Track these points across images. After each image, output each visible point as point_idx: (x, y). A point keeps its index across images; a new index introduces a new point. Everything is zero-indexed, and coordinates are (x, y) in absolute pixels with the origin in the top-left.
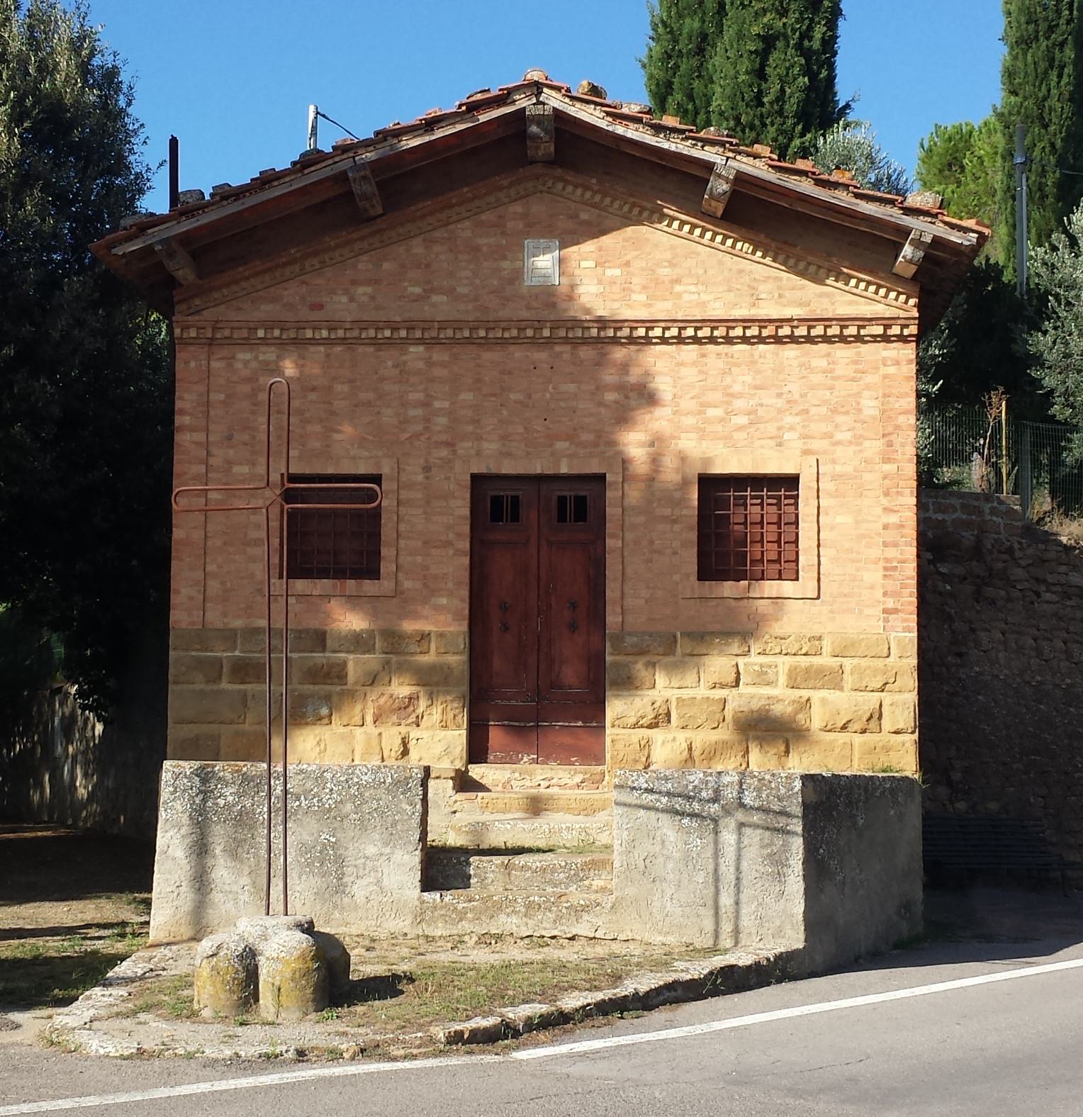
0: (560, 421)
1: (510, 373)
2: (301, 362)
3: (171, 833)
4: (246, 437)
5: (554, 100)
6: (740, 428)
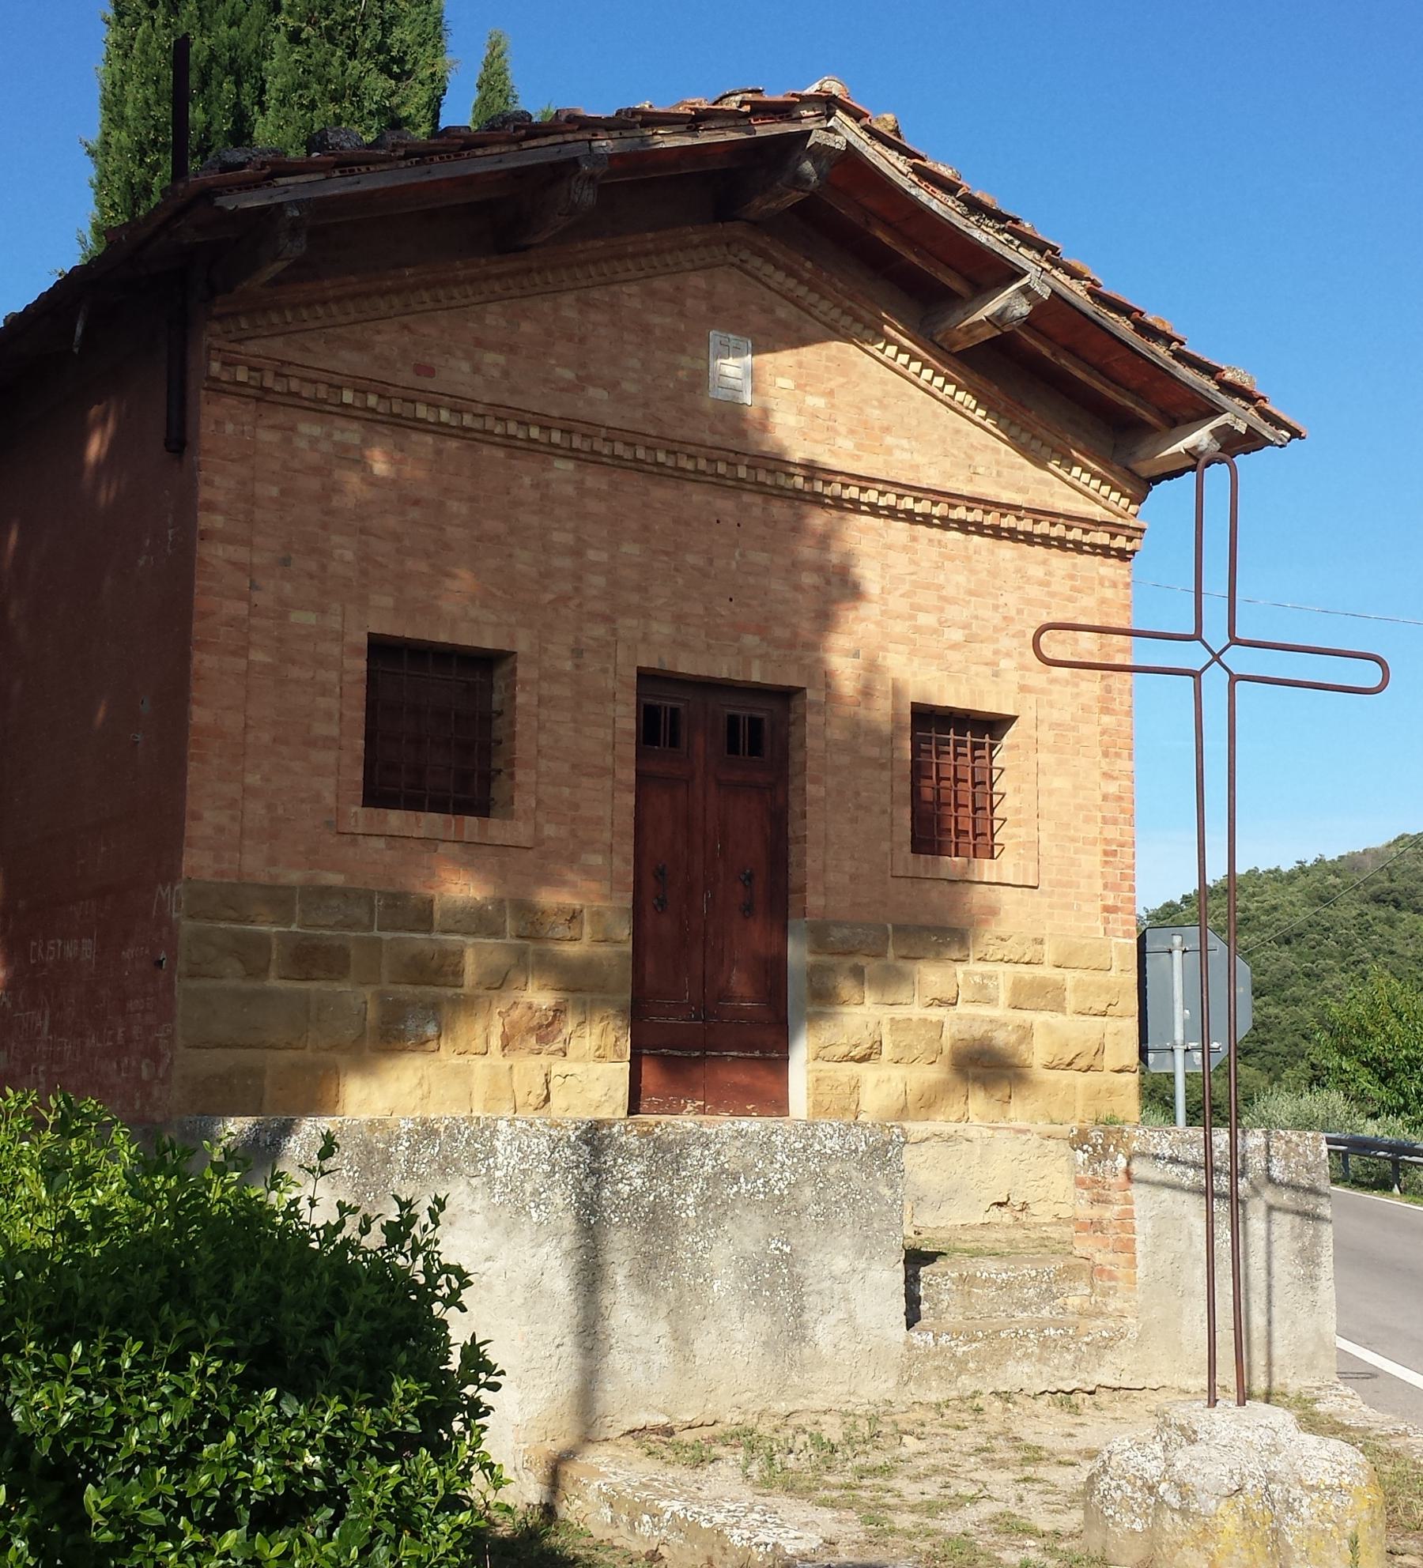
0: (748, 606)
1: (687, 524)
2: (398, 455)
3: (546, 1249)
4: (313, 566)
5: (846, 133)
6: (954, 647)
